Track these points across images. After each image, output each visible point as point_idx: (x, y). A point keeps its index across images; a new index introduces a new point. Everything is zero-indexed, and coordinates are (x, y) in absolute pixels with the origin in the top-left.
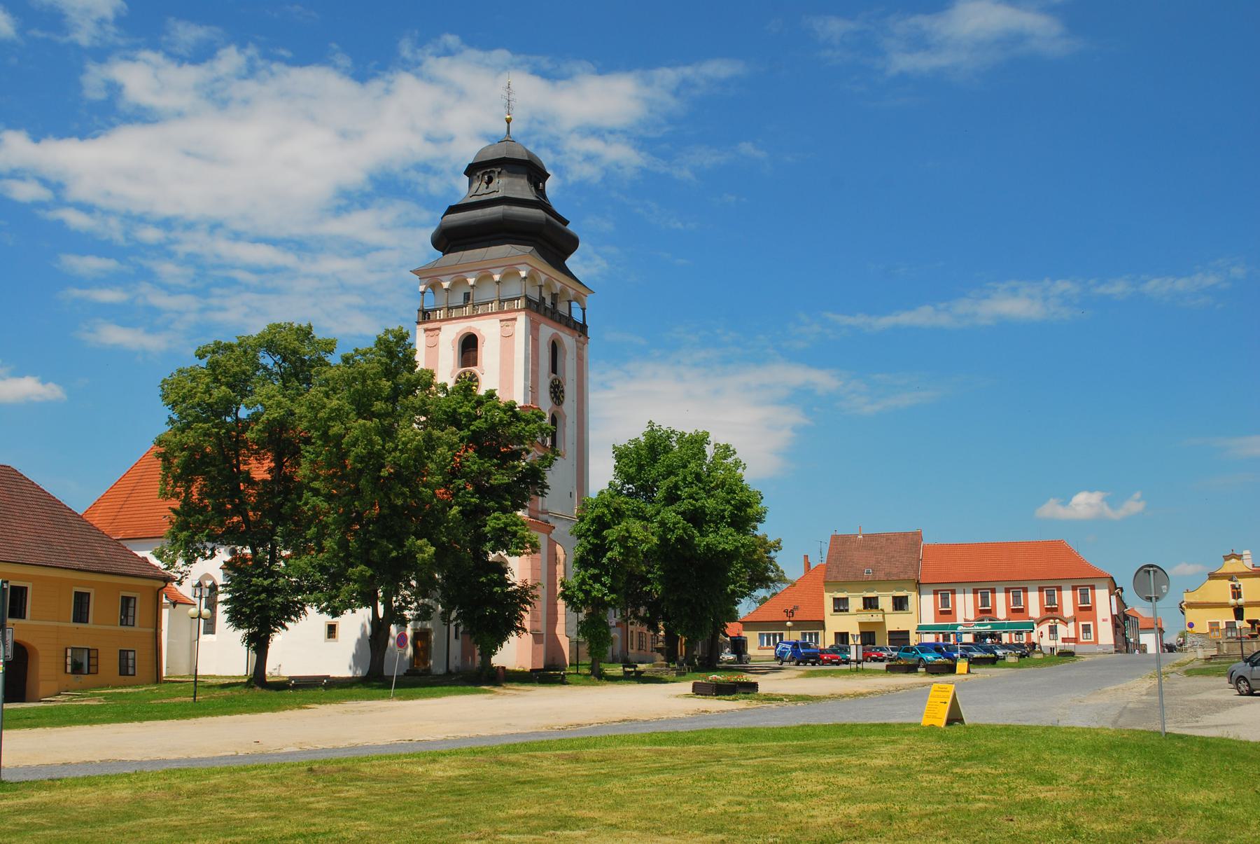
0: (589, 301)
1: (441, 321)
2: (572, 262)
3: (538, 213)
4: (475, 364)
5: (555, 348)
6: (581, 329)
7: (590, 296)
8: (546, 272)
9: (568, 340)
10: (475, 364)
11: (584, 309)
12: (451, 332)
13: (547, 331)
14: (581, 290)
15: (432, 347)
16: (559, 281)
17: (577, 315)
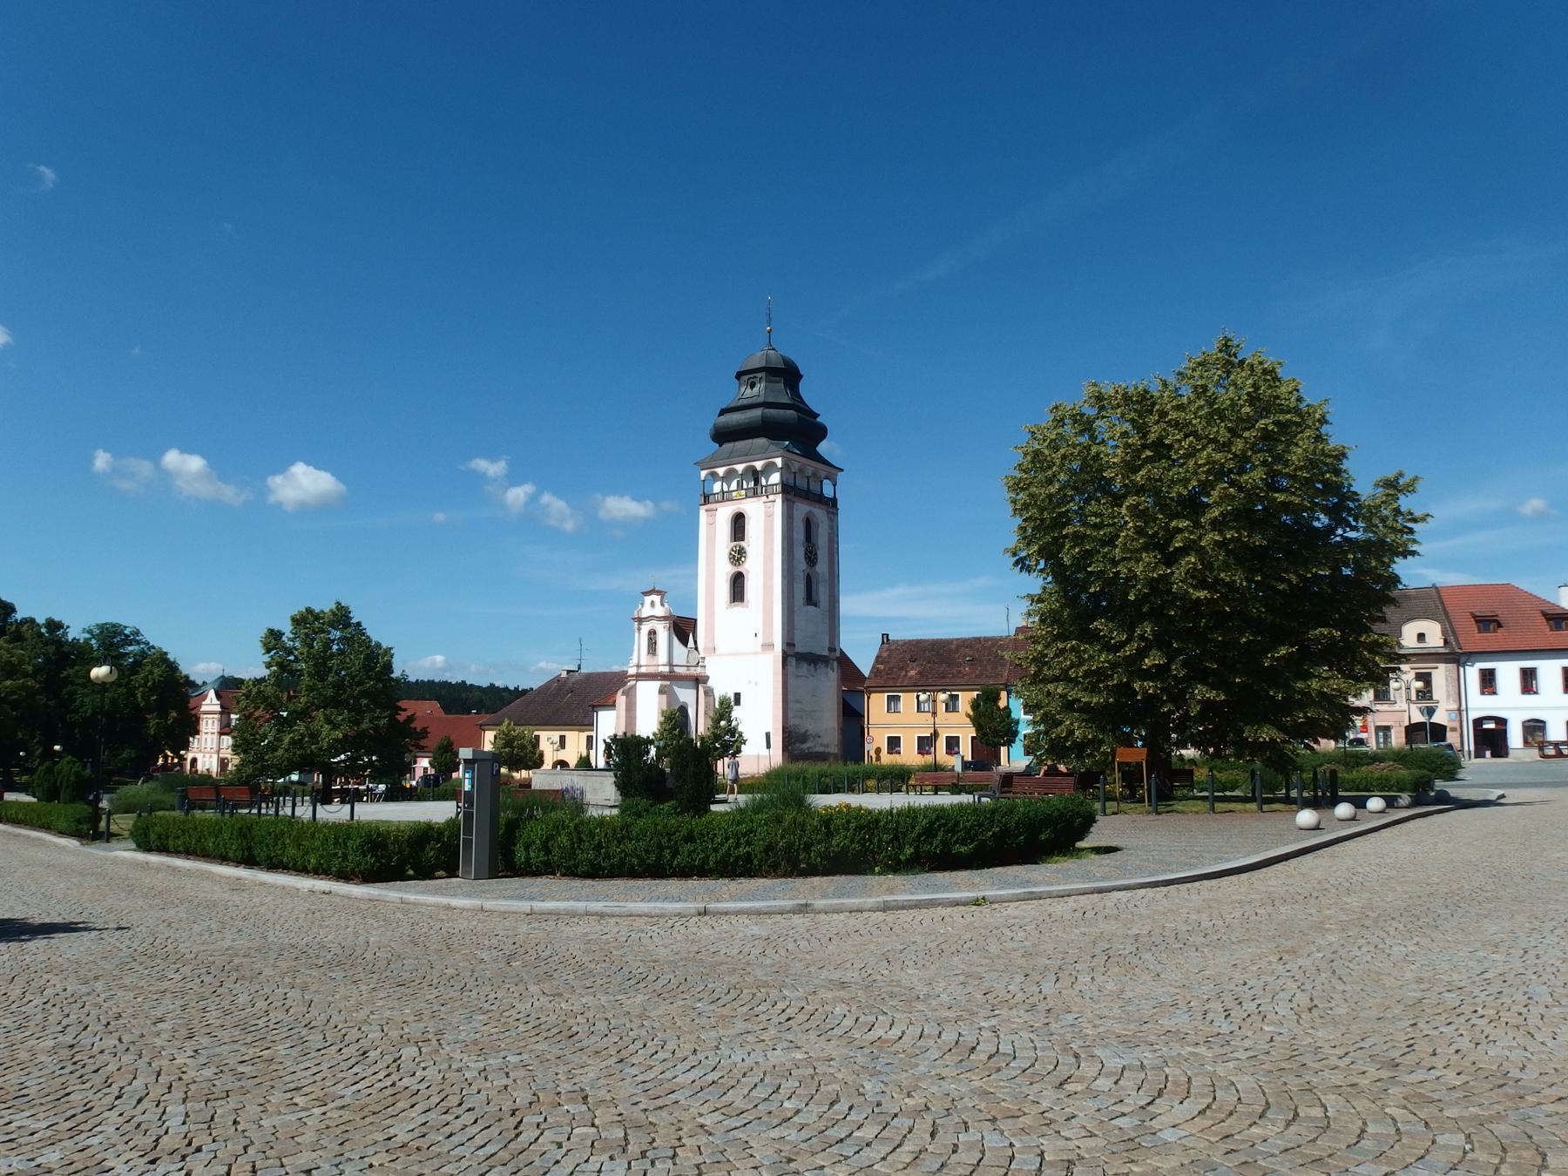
0: (840, 477)
1: (718, 502)
2: (823, 448)
3: (791, 413)
4: (743, 540)
5: (808, 524)
6: (833, 503)
7: (840, 474)
8: (799, 462)
9: (820, 513)
10: (743, 540)
11: (835, 486)
12: (725, 512)
13: (802, 509)
14: (833, 471)
15: (711, 524)
16: (811, 466)
17: (828, 490)
